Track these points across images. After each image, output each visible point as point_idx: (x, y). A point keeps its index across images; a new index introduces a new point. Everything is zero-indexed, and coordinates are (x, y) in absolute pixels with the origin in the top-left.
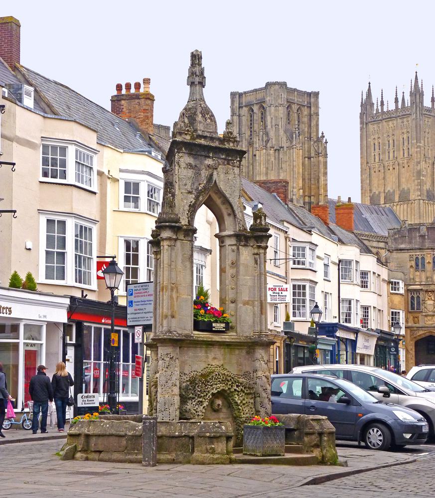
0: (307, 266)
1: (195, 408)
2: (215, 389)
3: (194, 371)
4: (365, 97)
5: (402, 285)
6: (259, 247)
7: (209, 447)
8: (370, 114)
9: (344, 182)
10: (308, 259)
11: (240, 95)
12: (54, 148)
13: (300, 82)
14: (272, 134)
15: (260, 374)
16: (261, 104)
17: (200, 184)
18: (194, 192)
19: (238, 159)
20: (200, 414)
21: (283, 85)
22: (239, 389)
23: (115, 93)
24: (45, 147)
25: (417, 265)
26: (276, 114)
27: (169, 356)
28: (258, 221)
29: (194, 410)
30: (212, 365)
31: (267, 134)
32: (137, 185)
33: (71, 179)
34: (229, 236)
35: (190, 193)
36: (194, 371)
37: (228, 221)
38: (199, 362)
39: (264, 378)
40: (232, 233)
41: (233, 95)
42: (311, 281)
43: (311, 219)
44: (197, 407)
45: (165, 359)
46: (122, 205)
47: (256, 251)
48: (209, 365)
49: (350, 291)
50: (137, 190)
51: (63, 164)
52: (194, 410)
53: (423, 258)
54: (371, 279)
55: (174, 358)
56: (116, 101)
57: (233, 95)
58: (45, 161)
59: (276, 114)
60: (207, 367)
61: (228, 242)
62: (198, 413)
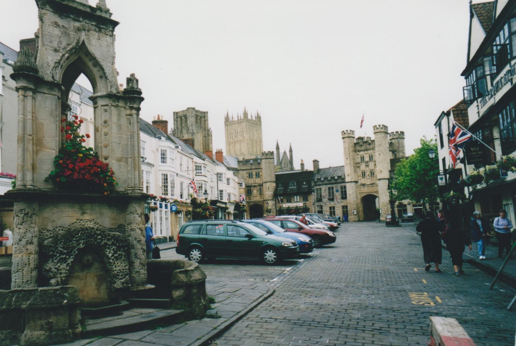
0: (203, 174)
1: (57, 267)
2: (81, 245)
3: (60, 227)
5: (244, 184)
6: (132, 108)
7: (43, 322)
8: (227, 121)
10: (203, 172)
11: (177, 113)
13: (201, 108)
14: (190, 128)
15: (134, 226)
16: (185, 116)
17: (68, 44)
18: (61, 51)
19: (111, 29)
20: (63, 271)
21: (194, 109)
22: (110, 243)
25: (249, 176)
26: (191, 120)
27: (23, 212)
28: (130, 85)
29: (56, 268)
30: (81, 220)
31: (188, 128)
34: (102, 97)
35: (56, 51)
36: (60, 227)
37: (100, 84)
38: (67, 217)
39: (138, 230)
40: (105, 94)
41: (174, 113)
42: (205, 181)
43: (204, 156)
44: (59, 264)
45: (19, 215)
47: (128, 112)
48: (77, 220)
49: (223, 186)
52: (56, 268)
53: (252, 173)
54: (231, 181)
55: (30, 214)
57: (174, 113)
59: (191, 120)
60: (76, 222)
61: (101, 102)
62: (60, 271)
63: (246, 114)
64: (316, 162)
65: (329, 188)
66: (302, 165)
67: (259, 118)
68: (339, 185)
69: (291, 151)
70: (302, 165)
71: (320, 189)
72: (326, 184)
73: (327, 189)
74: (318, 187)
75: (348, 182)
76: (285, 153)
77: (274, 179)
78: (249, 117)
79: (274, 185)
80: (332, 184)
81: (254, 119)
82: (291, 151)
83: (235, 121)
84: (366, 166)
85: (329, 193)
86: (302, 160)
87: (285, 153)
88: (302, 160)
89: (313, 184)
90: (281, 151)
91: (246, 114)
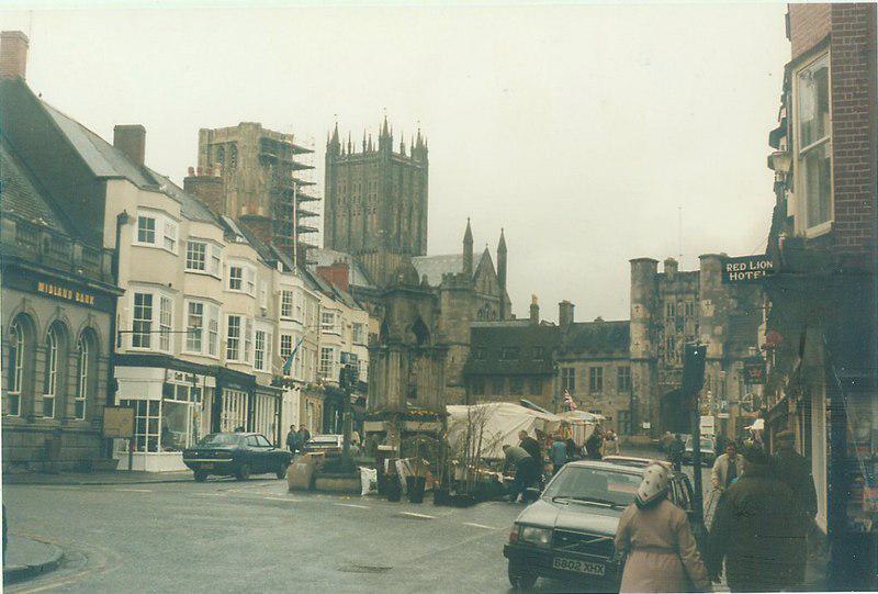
4: (331, 137)
9: (314, 233)
11: (211, 132)
12: (196, 245)
13: (273, 124)
16: (233, 145)
21: (257, 126)
23: (187, 175)
24: (190, 244)
32: (240, 270)
33: (208, 269)
41: (202, 132)
46: (228, 289)
50: (239, 275)
51: (202, 258)
56: (186, 181)
57: (202, 132)
58: (189, 254)
63: (386, 139)
64: (566, 308)
65: (592, 369)
66: (534, 308)
67: (421, 151)
68: (616, 365)
69: (502, 250)
70: (534, 308)
71: (572, 371)
72: (587, 360)
73: (587, 370)
74: (566, 365)
75: (636, 360)
76: (487, 253)
77: (466, 339)
78: (396, 149)
79: (467, 350)
80: (601, 360)
81: (408, 154)
82: (502, 250)
83: (358, 156)
84: (677, 327)
85: (592, 379)
86: (534, 298)
87: (487, 253)
88: (534, 298)
89: (555, 356)
90: (478, 249)
91: (386, 139)
